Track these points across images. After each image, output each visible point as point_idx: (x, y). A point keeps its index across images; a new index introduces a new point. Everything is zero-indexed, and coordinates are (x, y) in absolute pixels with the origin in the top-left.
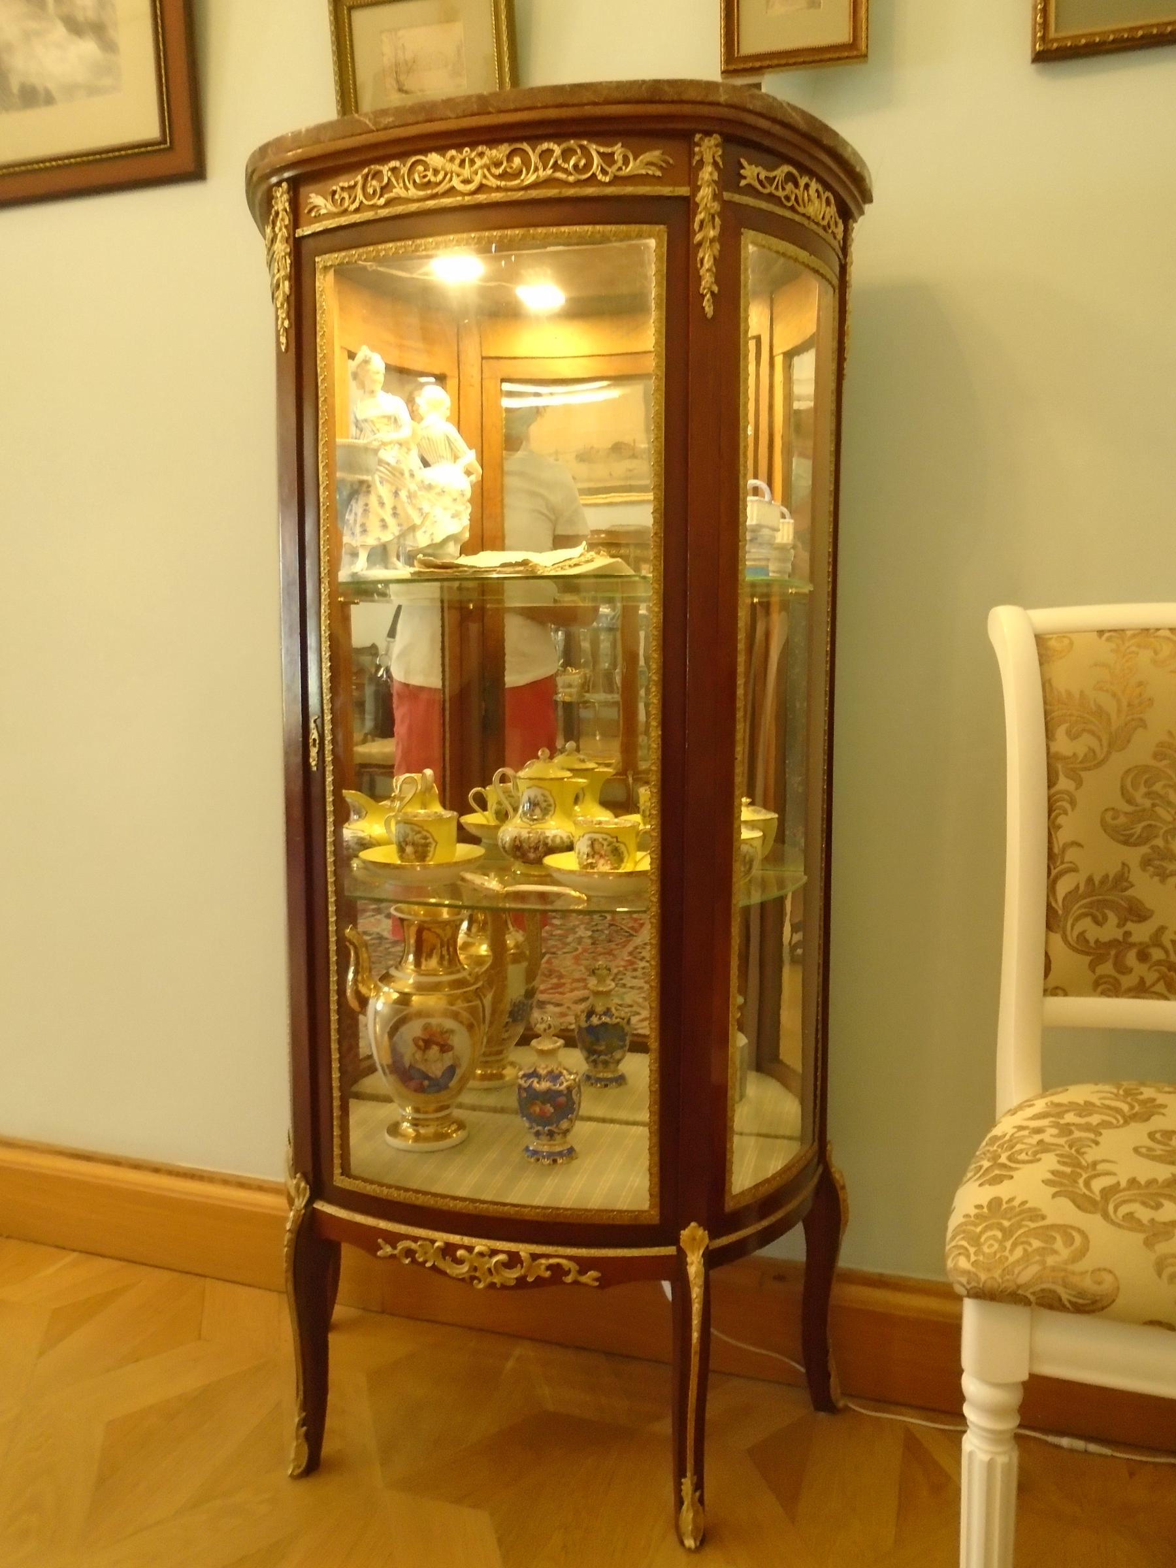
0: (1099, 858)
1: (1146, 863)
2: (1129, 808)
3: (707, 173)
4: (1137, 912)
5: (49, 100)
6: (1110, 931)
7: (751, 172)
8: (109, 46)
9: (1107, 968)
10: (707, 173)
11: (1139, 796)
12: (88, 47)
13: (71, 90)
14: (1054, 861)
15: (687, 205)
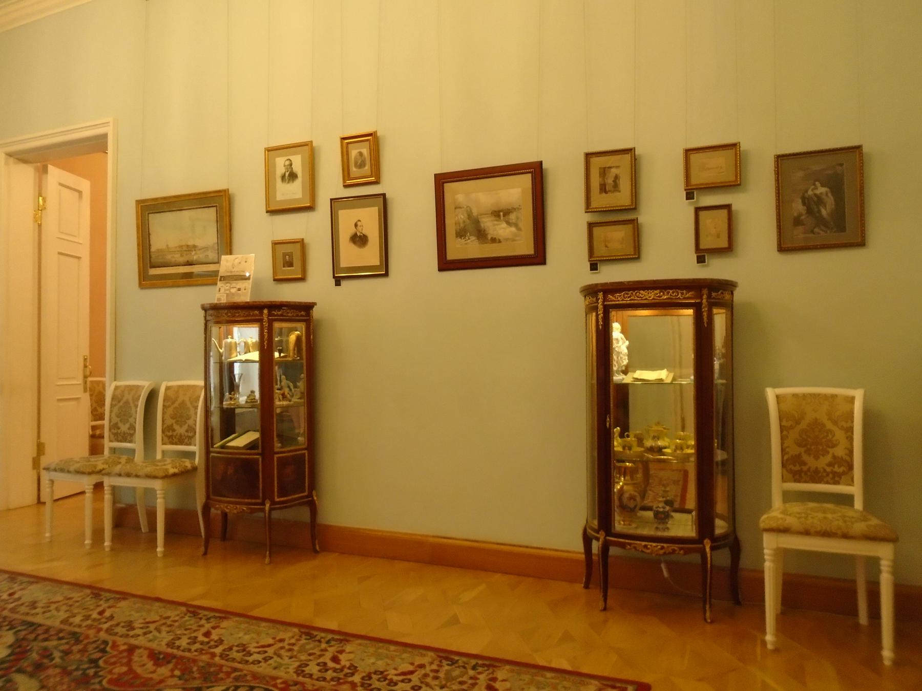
0: (794, 450)
1: (805, 452)
3: (705, 296)
4: (804, 464)
5: (500, 241)
6: (797, 468)
7: (714, 294)
8: (519, 229)
9: (797, 477)
10: (705, 296)
12: (513, 229)
13: (507, 239)
14: (783, 450)
15: (700, 304)
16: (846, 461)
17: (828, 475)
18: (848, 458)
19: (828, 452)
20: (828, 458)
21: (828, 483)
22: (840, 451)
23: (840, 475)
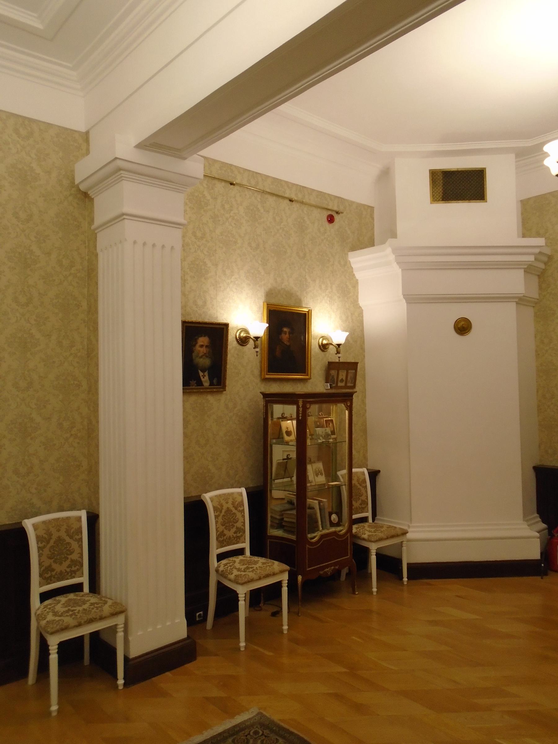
9: (49, 581)
17: (68, 574)
18: (80, 559)
19: (68, 558)
22: (75, 556)
23: (75, 572)
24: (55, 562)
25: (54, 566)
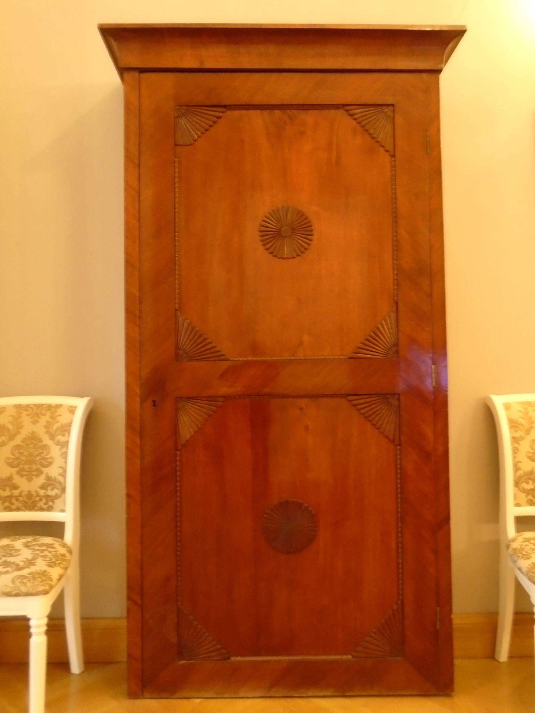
1: (18, 472)
2: (13, 457)
4: (15, 487)
6: (7, 493)
9: (7, 504)
11: (16, 453)
16: (60, 483)
19: (41, 472)
20: (41, 480)
21: (42, 509)
24: (20, 473)
25: (18, 480)
